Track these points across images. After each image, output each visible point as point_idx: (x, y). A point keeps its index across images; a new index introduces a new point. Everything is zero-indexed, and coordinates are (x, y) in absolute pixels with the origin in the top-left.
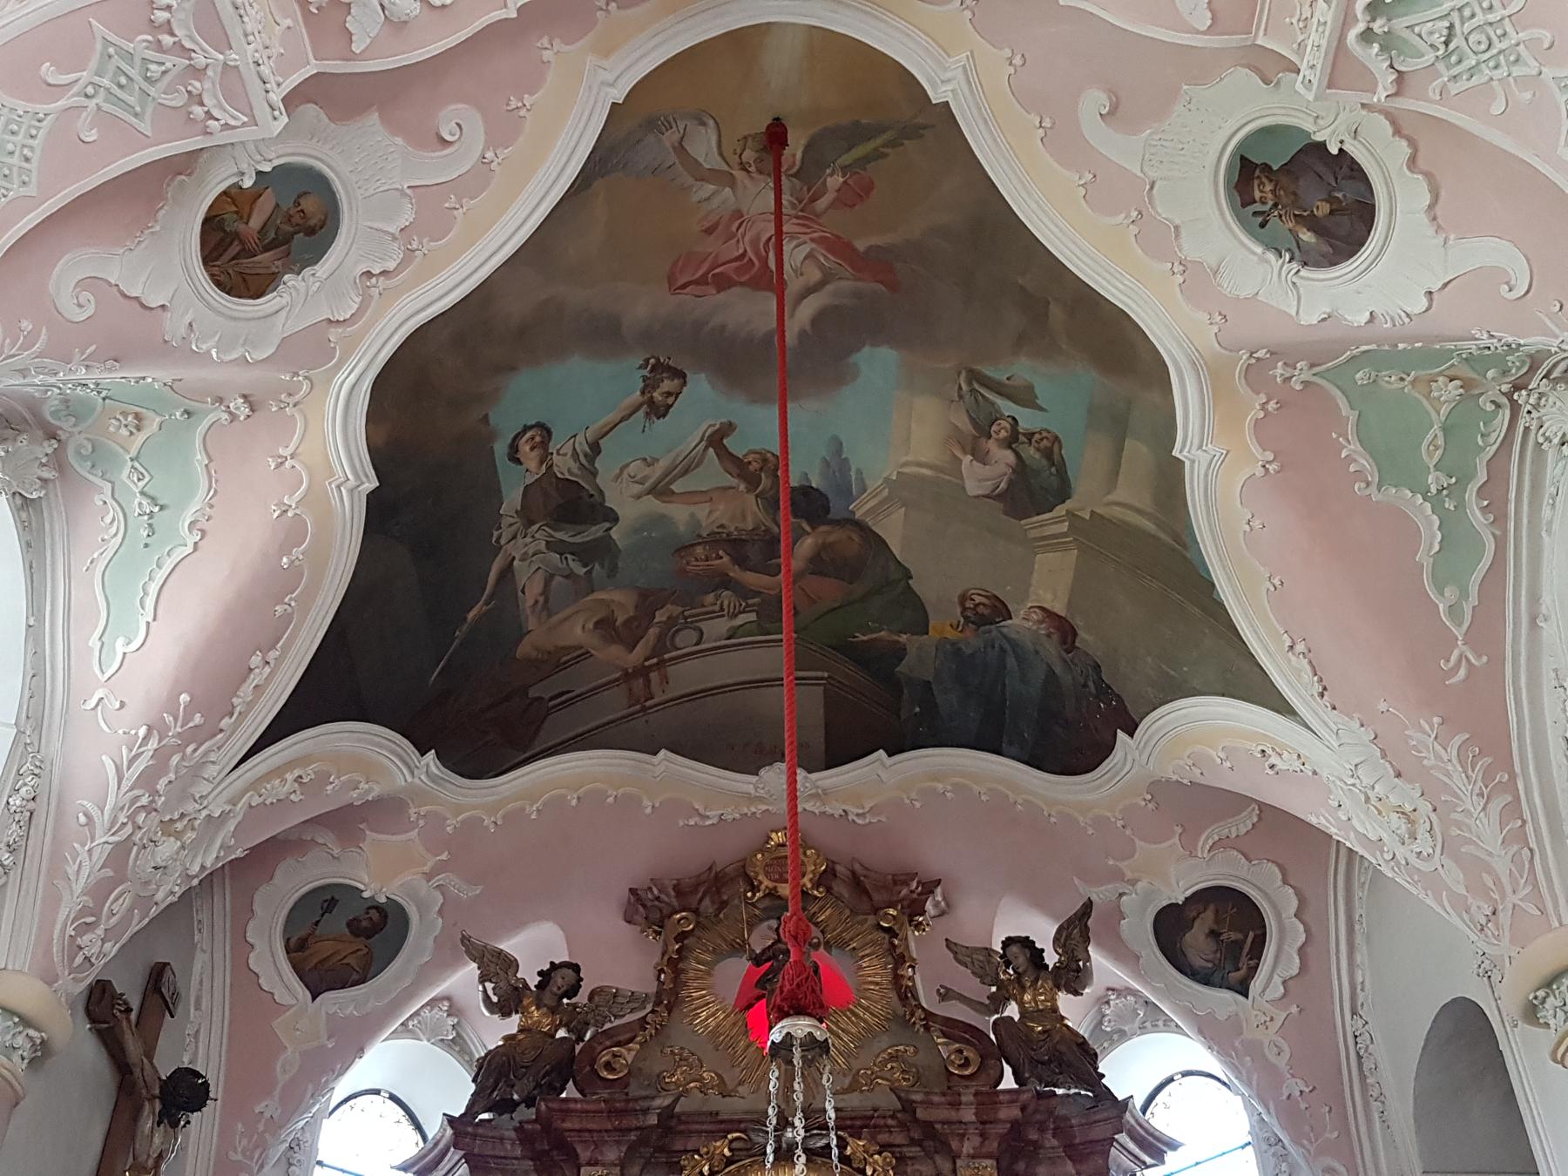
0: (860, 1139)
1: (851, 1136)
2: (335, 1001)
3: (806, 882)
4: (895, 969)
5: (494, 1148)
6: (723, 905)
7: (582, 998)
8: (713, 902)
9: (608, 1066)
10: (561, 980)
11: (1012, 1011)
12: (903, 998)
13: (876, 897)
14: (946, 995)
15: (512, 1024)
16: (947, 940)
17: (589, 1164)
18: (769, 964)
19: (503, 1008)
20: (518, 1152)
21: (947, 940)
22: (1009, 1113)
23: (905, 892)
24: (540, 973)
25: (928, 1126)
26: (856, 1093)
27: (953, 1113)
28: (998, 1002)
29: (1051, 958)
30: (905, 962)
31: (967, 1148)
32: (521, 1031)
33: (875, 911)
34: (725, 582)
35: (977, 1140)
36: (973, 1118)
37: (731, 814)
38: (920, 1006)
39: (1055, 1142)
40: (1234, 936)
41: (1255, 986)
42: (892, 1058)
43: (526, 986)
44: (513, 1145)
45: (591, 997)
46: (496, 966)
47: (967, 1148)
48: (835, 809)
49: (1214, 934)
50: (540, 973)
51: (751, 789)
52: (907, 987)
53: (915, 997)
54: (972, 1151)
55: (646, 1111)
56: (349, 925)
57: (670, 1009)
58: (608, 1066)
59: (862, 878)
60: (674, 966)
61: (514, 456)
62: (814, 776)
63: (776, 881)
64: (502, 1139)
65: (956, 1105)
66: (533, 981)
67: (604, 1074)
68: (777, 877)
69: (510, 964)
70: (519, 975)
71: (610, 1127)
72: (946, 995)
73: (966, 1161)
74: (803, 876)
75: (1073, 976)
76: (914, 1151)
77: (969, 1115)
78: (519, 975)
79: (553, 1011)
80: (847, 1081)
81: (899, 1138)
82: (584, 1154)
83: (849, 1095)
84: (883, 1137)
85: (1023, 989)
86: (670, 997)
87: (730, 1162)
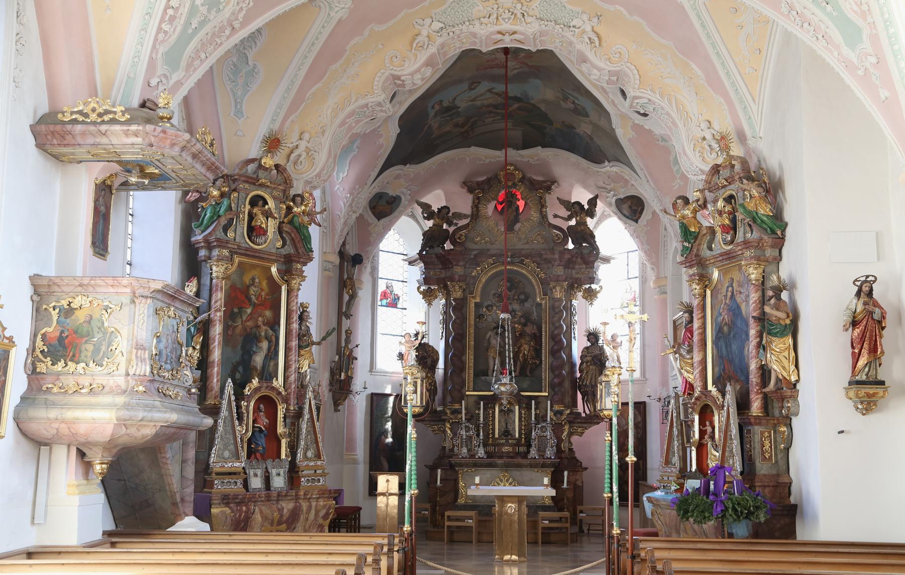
2: (383, 221)
3: (516, 180)
6: (491, 186)
7: (450, 214)
9: (459, 238)
10: (444, 211)
11: (573, 222)
12: (543, 218)
13: (537, 186)
14: (556, 216)
15: (430, 224)
17: (456, 265)
19: (428, 219)
20: (436, 260)
22: (567, 256)
23: (545, 184)
24: (438, 209)
25: (546, 259)
28: (569, 218)
29: (586, 207)
31: (556, 264)
33: (537, 190)
34: (492, 112)
35: (559, 262)
37: (493, 160)
38: (547, 221)
40: (635, 208)
41: (640, 221)
42: (539, 235)
43: (434, 212)
45: (453, 214)
46: (426, 207)
47: (556, 264)
48: (526, 160)
49: (630, 207)
50: (438, 209)
51: (499, 155)
53: (547, 218)
55: (470, 254)
56: (386, 202)
57: (475, 220)
58: (459, 238)
60: (476, 206)
61: (433, 108)
62: (519, 152)
64: (432, 257)
65: (554, 254)
66: (436, 210)
69: (430, 206)
72: (556, 216)
75: (591, 213)
76: (542, 262)
77: (557, 256)
79: (442, 220)
80: (526, 241)
81: (538, 259)
82: (455, 263)
84: (534, 259)
85: (577, 216)
86: (475, 215)
87: (493, 264)
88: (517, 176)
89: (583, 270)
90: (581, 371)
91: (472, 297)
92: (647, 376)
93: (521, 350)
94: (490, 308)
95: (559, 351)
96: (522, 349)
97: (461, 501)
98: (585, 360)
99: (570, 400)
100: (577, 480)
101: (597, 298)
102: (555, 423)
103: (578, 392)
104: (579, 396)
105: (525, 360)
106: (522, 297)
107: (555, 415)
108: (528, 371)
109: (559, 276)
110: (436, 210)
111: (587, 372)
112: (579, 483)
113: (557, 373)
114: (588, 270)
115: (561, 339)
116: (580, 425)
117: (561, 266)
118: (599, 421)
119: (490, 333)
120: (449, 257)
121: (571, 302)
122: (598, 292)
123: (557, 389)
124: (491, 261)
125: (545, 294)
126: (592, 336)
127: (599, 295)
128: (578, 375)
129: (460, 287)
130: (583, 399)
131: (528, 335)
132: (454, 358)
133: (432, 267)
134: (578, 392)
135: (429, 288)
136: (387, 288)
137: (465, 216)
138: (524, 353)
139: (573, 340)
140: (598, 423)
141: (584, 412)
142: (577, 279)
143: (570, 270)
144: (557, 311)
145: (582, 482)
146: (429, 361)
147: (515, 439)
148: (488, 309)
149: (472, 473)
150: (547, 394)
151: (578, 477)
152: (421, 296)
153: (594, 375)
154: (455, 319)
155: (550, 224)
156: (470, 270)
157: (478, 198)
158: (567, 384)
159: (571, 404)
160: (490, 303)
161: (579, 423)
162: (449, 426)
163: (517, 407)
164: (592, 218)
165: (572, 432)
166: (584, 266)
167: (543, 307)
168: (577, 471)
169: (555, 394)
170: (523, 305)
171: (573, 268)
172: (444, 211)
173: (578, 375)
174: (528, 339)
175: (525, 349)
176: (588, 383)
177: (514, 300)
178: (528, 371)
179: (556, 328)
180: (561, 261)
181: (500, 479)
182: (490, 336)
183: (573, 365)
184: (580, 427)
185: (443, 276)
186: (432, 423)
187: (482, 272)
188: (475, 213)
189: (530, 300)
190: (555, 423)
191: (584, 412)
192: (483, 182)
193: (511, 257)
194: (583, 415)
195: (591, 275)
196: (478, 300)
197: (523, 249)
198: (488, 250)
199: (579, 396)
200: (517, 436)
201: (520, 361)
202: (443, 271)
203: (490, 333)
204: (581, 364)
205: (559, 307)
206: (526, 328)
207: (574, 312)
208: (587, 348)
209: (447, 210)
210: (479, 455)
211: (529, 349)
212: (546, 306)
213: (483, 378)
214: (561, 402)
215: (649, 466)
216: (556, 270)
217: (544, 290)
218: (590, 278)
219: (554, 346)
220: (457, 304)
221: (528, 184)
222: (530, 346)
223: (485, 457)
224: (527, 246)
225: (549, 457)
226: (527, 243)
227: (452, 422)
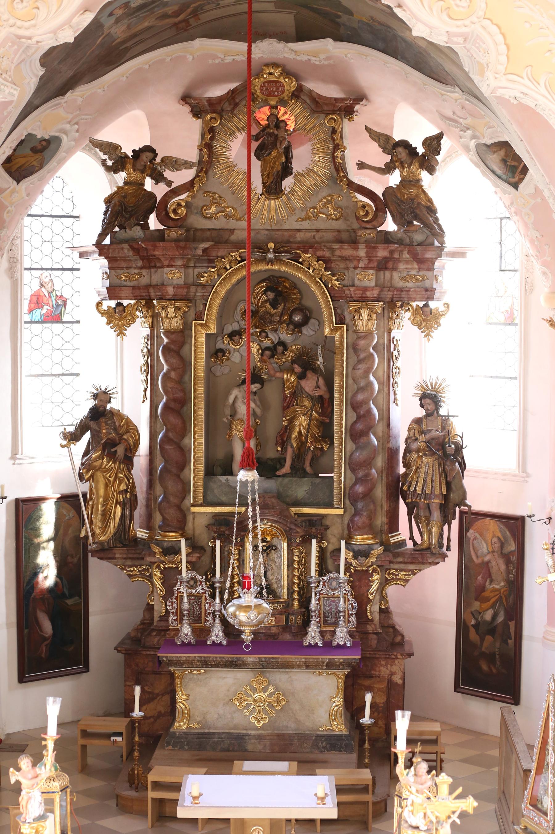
0: (307, 254)
1: (303, 252)
4: (334, 152)
5: (119, 252)
6: (236, 105)
8: (230, 105)
9: (175, 211)
12: (337, 170)
14: (361, 165)
15: (121, 177)
16: (366, 126)
17: (168, 266)
18: (262, 139)
19: (114, 169)
21: (366, 126)
24: (134, 151)
26: (308, 221)
27: (354, 252)
30: (339, 149)
31: (361, 265)
32: (126, 183)
35: (366, 262)
36: (365, 255)
38: (346, 176)
39: (408, 256)
44: (128, 250)
45: (162, 160)
47: (361, 265)
52: (340, 163)
53: (345, 170)
54: (363, 266)
57: (206, 173)
58: (175, 211)
59: (317, 99)
63: (267, 95)
66: (130, 154)
67: (172, 216)
68: (267, 93)
70: (122, 151)
71: (178, 254)
72: (361, 165)
73: (360, 271)
74: (283, 92)
78: (122, 151)
79: (142, 172)
83: (304, 222)
84: (320, 253)
88: (287, 88)
89: (413, 273)
90: (406, 465)
91: (202, 325)
92: (529, 470)
93: (294, 426)
94: (236, 338)
95: (365, 433)
96: (297, 423)
97: (180, 725)
98: (414, 446)
99: (385, 519)
100: (392, 674)
101: (439, 325)
102: (355, 570)
103: (401, 501)
104: (403, 509)
105: (302, 444)
106: (297, 318)
107: (355, 557)
108: (307, 463)
109: (366, 289)
110: (130, 154)
111: (417, 469)
112: (397, 679)
113: (361, 474)
114: (421, 273)
115: (369, 411)
116: (402, 566)
117: (372, 268)
118: (437, 561)
119: (235, 392)
120: (156, 253)
121: (390, 332)
122: (441, 315)
123: (360, 505)
124: (236, 255)
125: (341, 320)
126: (428, 401)
127: (442, 320)
128: (402, 470)
129: (177, 309)
130: (410, 514)
131: (309, 396)
132: (167, 447)
133: (124, 265)
134: (401, 501)
135: (119, 304)
136: (42, 285)
137: (188, 165)
138: (300, 432)
139: (392, 405)
140: (437, 564)
141: (412, 538)
142: (401, 290)
143: (388, 274)
144: (362, 356)
145: (403, 679)
146: (120, 450)
147: (281, 603)
148: (231, 339)
149: (200, 677)
150: (341, 511)
151: (395, 668)
152: (104, 320)
153: (429, 476)
154: (168, 371)
155: (351, 184)
156: (197, 271)
157: (212, 130)
158: (380, 492)
159: (386, 527)
160: (236, 327)
161: (400, 563)
162: (159, 575)
163: (285, 545)
164: (431, 174)
165: (387, 580)
166: (416, 266)
167: (337, 343)
168: (393, 658)
169: (356, 513)
170: (300, 332)
171: (396, 269)
172: (148, 156)
173: (402, 470)
174: (307, 403)
175: (301, 424)
176: (419, 490)
177: (281, 323)
178: (307, 463)
179: (360, 389)
180: (370, 261)
181: (250, 686)
182: (236, 398)
183: (392, 454)
184: (402, 570)
185: (144, 281)
186: (129, 563)
187: (219, 276)
188: (206, 158)
189: (312, 321)
190: (355, 570)
191: (412, 538)
192: (220, 99)
193: (275, 251)
194: (410, 545)
195: (427, 283)
196: (213, 329)
197: (299, 230)
198: (232, 231)
199: (403, 509)
200: (285, 597)
201: (292, 446)
202: (144, 272)
203: (235, 392)
204: (407, 451)
205: (366, 349)
206: (303, 383)
207: (395, 353)
208: (418, 421)
209: (150, 155)
210: (214, 638)
211: (309, 425)
212: (342, 343)
213: (223, 479)
214: (370, 528)
215: (526, 632)
216: (360, 276)
217: (339, 311)
218: (426, 290)
219: (355, 423)
220: (172, 342)
221: (308, 101)
222: (311, 419)
223: (224, 643)
224: (306, 225)
225: (341, 643)
226: (307, 218)
227: (165, 568)
